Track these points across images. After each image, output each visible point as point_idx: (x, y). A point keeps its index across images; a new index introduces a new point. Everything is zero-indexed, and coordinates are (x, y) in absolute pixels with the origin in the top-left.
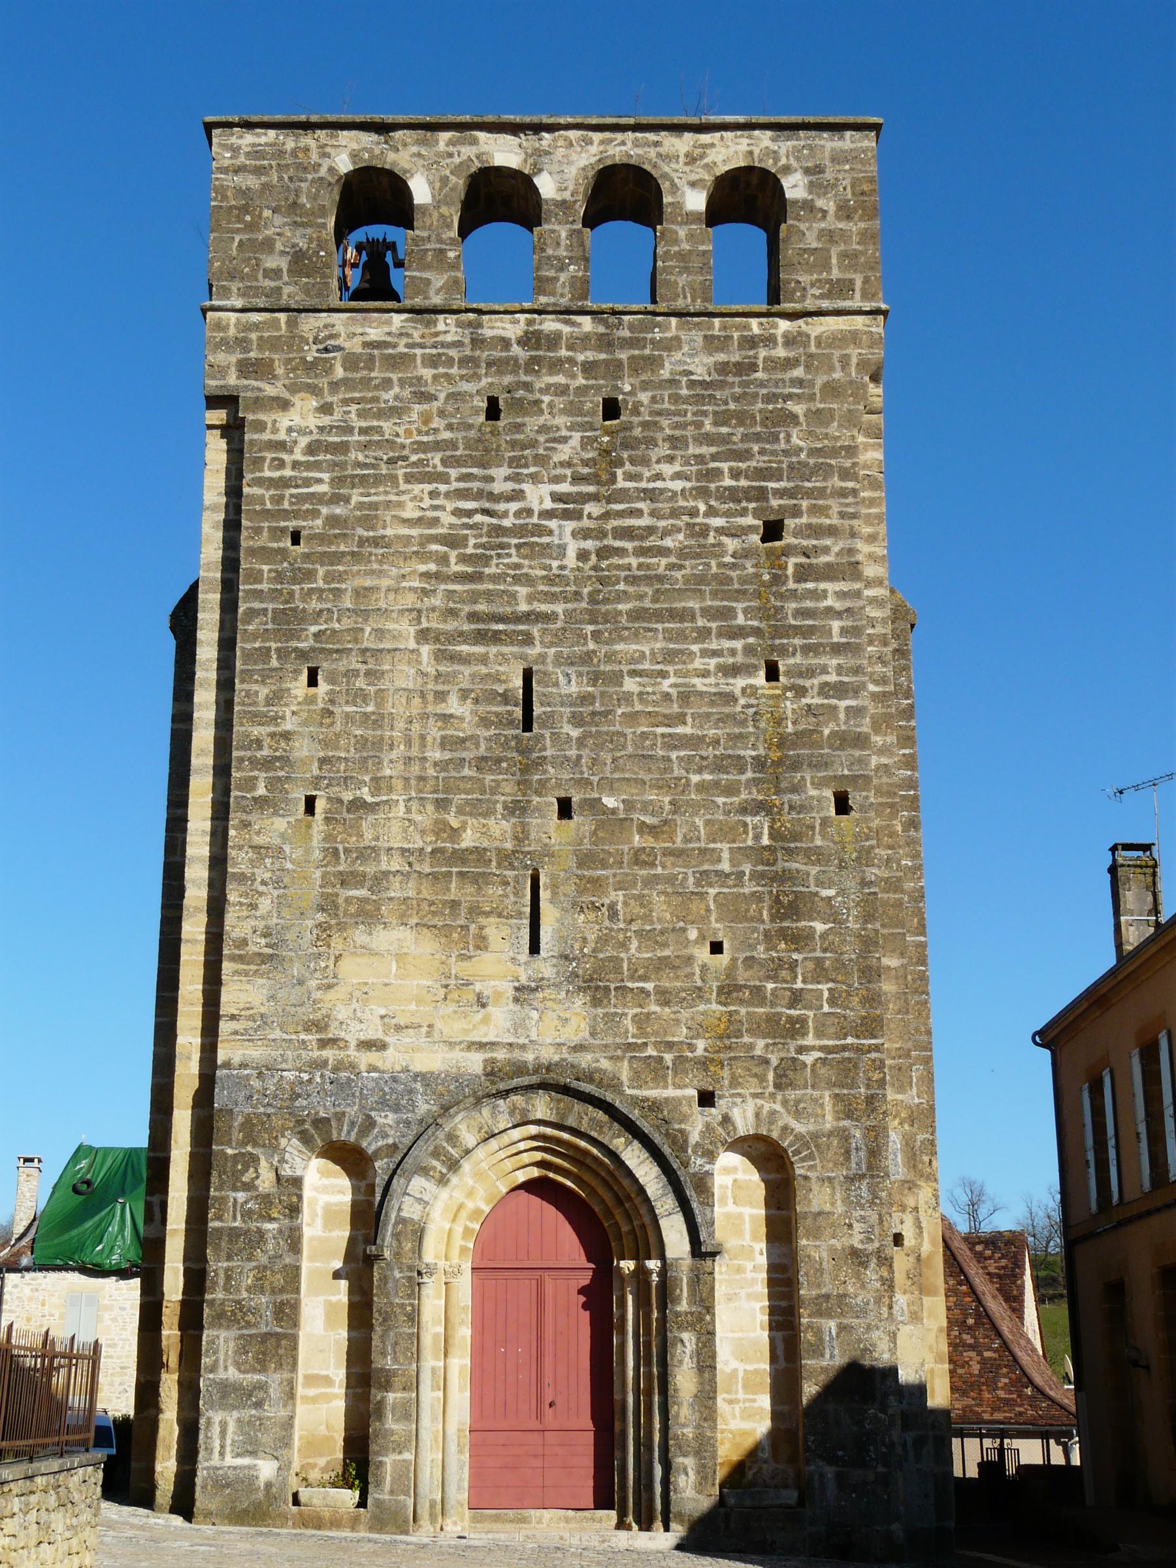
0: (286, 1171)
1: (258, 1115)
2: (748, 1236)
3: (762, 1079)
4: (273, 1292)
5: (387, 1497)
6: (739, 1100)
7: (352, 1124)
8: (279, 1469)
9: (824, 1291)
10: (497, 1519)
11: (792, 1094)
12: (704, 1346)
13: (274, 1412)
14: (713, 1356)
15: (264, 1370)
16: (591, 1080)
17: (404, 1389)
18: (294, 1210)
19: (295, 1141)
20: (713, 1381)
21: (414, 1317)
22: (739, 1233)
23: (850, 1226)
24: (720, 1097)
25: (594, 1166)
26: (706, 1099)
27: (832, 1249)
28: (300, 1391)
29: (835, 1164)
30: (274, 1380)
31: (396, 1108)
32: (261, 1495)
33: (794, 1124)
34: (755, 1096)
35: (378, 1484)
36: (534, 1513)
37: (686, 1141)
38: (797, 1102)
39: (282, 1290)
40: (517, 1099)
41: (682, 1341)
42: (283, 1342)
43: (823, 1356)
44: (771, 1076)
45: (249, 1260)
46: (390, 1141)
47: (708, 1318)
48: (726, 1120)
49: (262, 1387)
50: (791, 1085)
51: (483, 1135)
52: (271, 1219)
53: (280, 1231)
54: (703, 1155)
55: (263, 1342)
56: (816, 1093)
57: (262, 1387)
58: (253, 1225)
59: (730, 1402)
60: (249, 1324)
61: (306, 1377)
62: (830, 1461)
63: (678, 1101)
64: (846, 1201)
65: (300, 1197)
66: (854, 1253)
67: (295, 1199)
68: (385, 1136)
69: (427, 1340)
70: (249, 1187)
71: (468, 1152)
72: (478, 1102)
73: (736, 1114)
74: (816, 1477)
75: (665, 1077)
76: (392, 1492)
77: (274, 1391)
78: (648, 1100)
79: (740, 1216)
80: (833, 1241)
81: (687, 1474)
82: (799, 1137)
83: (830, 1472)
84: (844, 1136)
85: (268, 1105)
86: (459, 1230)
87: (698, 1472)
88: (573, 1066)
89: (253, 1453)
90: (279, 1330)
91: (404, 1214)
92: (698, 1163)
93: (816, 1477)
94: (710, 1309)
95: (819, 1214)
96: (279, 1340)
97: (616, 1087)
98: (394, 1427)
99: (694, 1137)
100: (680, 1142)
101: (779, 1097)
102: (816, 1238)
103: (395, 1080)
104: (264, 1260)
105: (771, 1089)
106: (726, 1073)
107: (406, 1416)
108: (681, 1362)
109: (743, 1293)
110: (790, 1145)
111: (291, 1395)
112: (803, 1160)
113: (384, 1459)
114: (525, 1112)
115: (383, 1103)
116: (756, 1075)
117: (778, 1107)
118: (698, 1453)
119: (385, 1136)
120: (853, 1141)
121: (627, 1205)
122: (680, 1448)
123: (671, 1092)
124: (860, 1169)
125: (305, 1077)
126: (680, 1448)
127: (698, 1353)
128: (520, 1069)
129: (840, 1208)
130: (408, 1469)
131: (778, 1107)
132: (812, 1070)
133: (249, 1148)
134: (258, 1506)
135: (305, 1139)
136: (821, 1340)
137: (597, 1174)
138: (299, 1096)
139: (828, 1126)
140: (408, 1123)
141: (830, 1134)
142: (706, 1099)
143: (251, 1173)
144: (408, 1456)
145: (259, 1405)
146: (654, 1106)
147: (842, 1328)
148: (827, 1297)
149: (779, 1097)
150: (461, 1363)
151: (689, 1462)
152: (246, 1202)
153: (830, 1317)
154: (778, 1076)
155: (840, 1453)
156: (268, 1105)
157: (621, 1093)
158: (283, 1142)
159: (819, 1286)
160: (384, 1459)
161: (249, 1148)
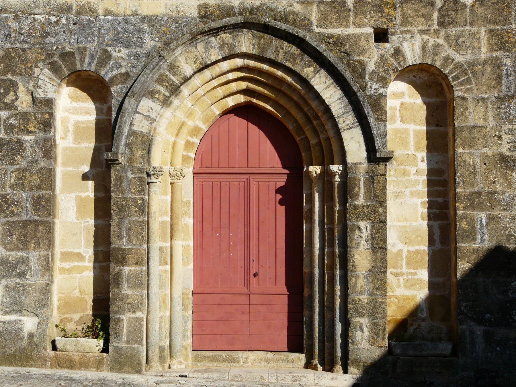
0: (40, 94)
1: (15, 50)
2: (412, 147)
3: (428, 18)
4: (31, 188)
5: (124, 345)
6: (408, 36)
7: (92, 57)
8: (39, 323)
9: (476, 189)
10: (213, 359)
11: (453, 31)
12: (378, 232)
13: (36, 280)
14: (385, 241)
15: (25, 248)
16: (287, 21)
17: (137, 264)
18: (47, 125)
19: (46, 71)
20: (384, 259)
21: (144, 208)
22: (405, 144)
23: (500, 137)
24: (393, 34)
25: (288, 92)
26: (381, 36)
27: (484, 156)
28: (58, 264)
29: (489, 87)
30: (34, 256)
31: (128, 45)
32: (25, 343)
33: (453, 54)
34: (422, 32)
35: (117, 336)
36: (242, 355)
37: (364, 70)
38: (458, 37)
39: (38, 187)
40: (226, 36)
41: (359, 228)
42: (40, 228)
43: (475, 240)
44: (435, 16)
45: (12, 164)
46: (123, 70)
47: (381, 210)
48: (398, 52)
49: (24, 261)
50: (452, 22)
51: (198, 65)
52: (29, 132)
53: (36, 142)
54: (378, 81)
55: (24, 227)
56: (474, 30)
57: (24, 261)
58: (15, 137)
59: (396, 275)
60: (12, 214)
61: (63, 254)
62: (480, 321)
63: (356, 38)
64: (498, 117)
65: (51, 115)
66: (503, 159)
67: (47, 116)
68: (120, 66)
69: (155, 226)
70: (10, 106)
71: (187, 80)
72: (193, 39)
73: (406, 48)
74: (468, 333)
75: (347, 18)
76: (128, 342)
77: (34, 265)
78: (333, 36)
79: (406, 131)
80: (485, 150)
81: (362, 330)
82: (458, 66)
83: (479, 330)
84: (497, 64)
85: (24, 41)
86: (181, 143)
87: (371, 329)
88: (271, 10)
89: (18, 312)
90: (37, 218)
91: (135, 128)
92: (373, 87)
93: (468, 333)
94: (382, 203)
95: (474, 127)
96: (37, 226)
97: (307, 26)
98: (129, 292)
99: (371, 66)
100: (359, 70)
101: (442, 33)
102: (471, 147)
103: (126, 21)
104: (24, 164)
105: (435, 26)
106: (398, 14)
107: (139, 284)
108: (358, 244)
109: (407, 191)
110: (451, 72)
111: (47, 267)
112: (461, 84)
113: (122, 317)
114: (232, 46)
115: (117, 40)
116: (423, 16)
117: (441, 41)
118: (371, 315)
119: (120, 66)
120: (504, 68)
121: (315, 123)
122: (357, 310)
123: (352, 30)
124: (510, 91)
125: (53, 19)
126: (357, 310)
127: (373, 237)
128: (228, 11)
129: (491, 123)
130: (141, 325)
131: (441, 41)
132: (471, 11)
133: (9, 76)
134: (23, 351)
135: (55, 69)
136: (474, 228)
137: (291, 99)
138: (48, 34)
139: (483, 56)
140: (137, 56)
141: (484, 63)
142: (381, 36)
143: (12, 96)
144: (141, 314)
145: (22, 275)
146: (338, 42)
147: (491, 219)
148: (479, 194)
149: (442, 33)
150: (184, 244)
151: (364, 321)
152: (8, 119)
153: (481, 209)
154: (441, 16)
155: (488, 316)
156: (24, 41)
157: (311, 31)
158: (37, 71)
159: (472, 185)
160: (122, 317)
161: (9, 76)
